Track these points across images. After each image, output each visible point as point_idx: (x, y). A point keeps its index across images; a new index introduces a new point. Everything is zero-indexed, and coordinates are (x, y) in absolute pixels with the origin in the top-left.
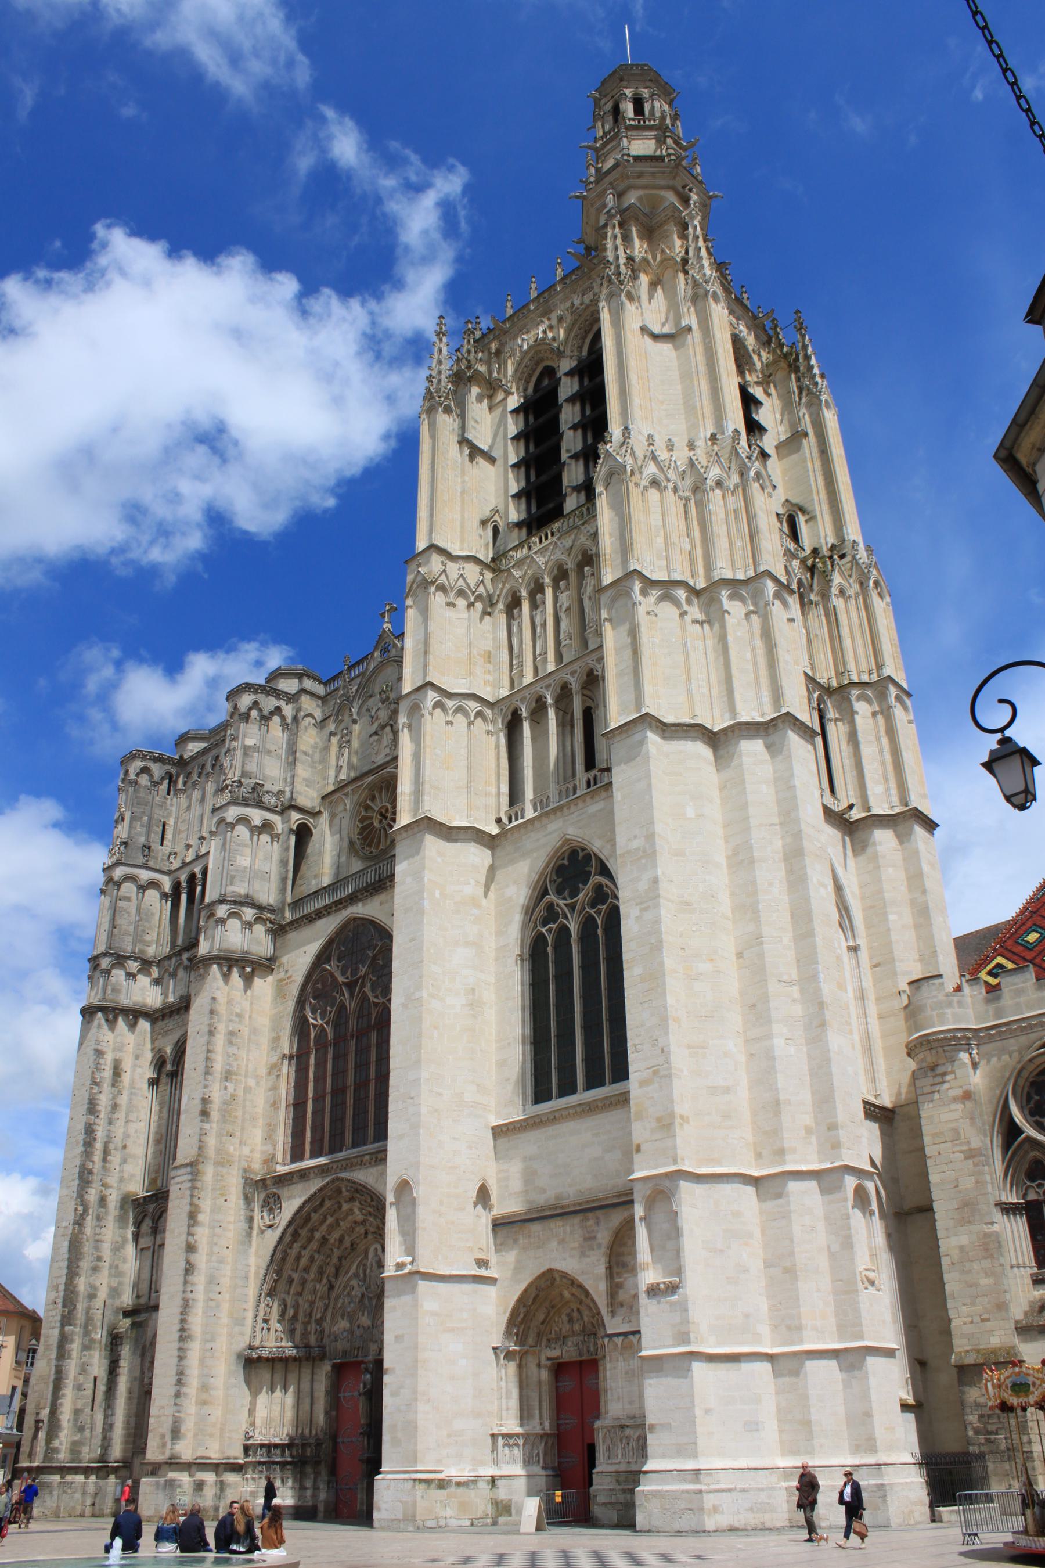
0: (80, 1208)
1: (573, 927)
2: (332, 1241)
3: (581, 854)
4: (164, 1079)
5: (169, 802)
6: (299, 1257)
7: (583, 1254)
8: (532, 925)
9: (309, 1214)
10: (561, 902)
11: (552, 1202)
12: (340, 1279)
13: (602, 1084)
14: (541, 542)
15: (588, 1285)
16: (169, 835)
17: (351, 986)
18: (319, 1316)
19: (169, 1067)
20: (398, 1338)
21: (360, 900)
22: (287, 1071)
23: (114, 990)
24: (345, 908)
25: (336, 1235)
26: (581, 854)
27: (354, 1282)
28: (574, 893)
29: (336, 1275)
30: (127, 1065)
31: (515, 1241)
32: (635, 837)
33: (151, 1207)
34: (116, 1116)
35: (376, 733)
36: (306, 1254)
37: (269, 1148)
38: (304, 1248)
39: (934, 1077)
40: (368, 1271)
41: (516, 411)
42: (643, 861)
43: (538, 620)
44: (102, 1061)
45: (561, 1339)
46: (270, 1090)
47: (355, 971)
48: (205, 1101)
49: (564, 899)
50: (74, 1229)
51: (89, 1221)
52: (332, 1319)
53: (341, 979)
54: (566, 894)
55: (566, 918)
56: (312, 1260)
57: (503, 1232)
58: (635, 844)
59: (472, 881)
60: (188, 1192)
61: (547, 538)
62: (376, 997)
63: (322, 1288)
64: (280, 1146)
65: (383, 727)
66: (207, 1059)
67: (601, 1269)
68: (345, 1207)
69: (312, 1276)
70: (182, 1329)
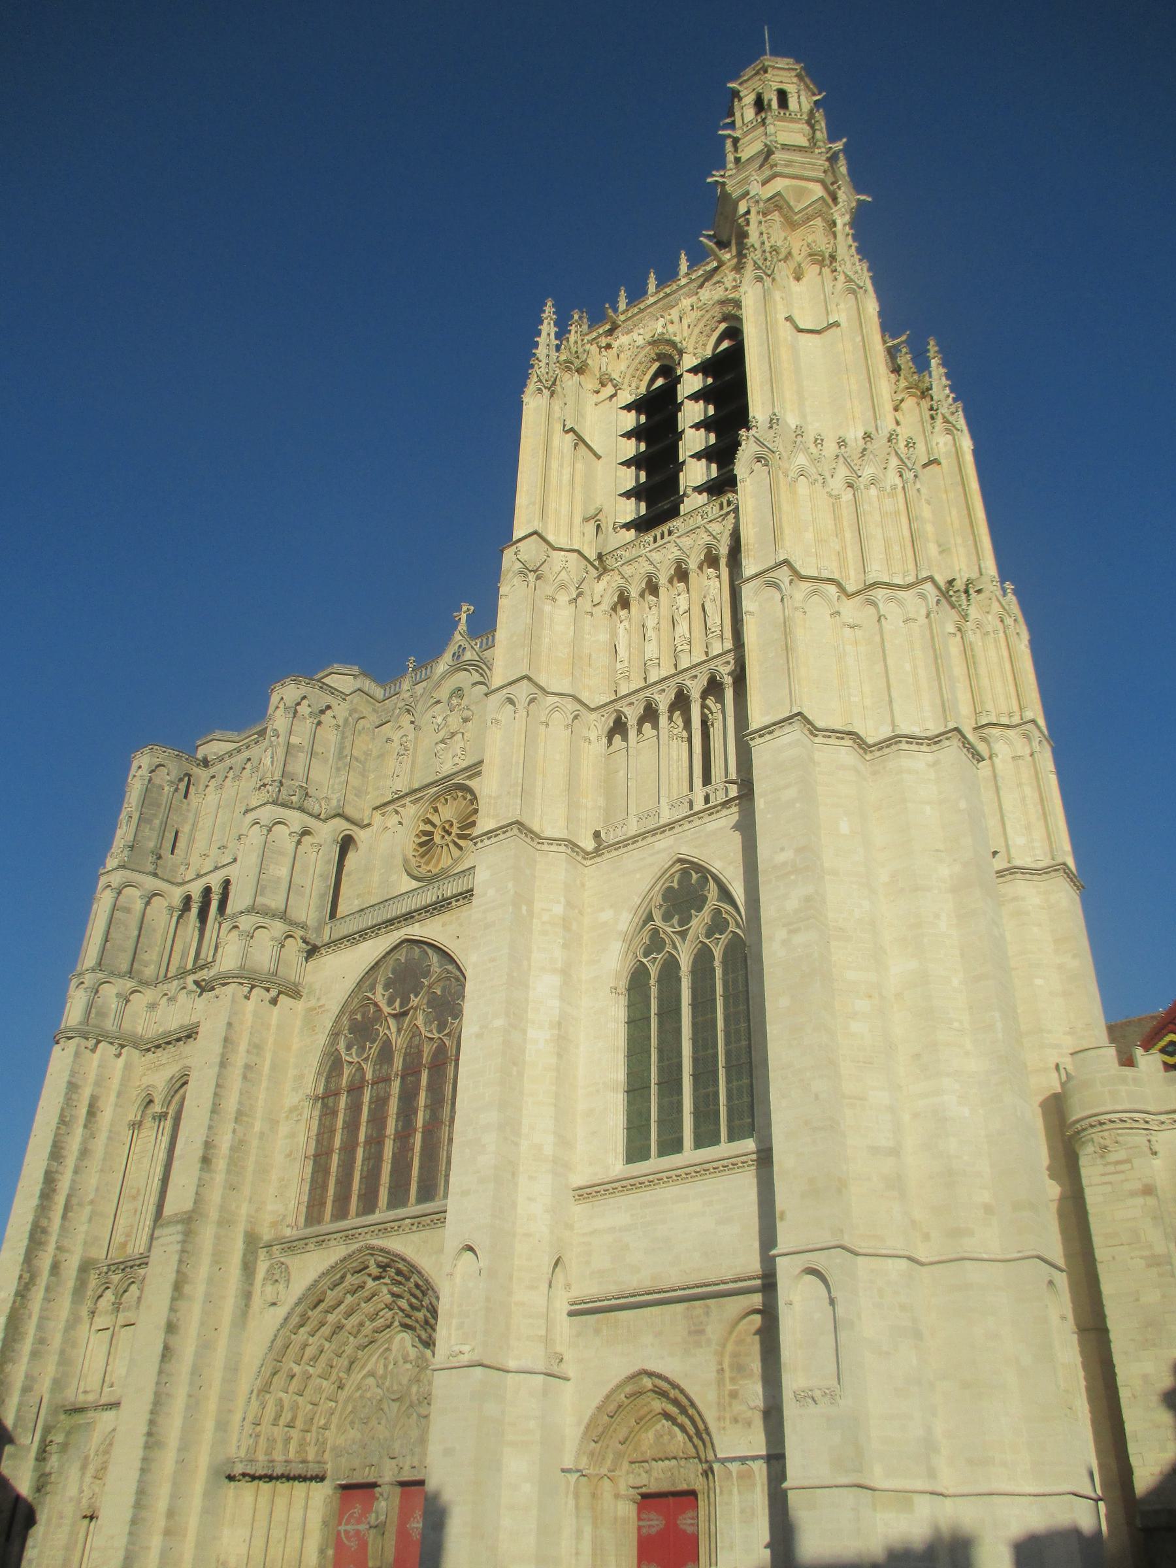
0: (26, 1276)
2: (348, 1327)
4: (149, 1123)
5: (185, 807)
6: (305, 1346)
9: (324, 1293)
10: (669, 930)
11: (648, 1284)
12: (353, 1376)
14: (655, 541)
16: (181, 844)
17: (399, 1016)
18: (322, 1422)
19: (157, 1108)
20: (448, 1452)
23: (98, 1014)
27: (371, 1381)
29: (349, 1369)
32: (782, 849)
33: (116, 1278)
34: (85, 1163)
35: (442, 742)
39: (1105, 1165)
40: (391, 1367)
41: (628, 408)
42: (793, 877)
43: (651, 623)
44: (74, 1096)
47: (405, 1001)
48: (208, 1145)
50: (14, 1302)
51: (38, 1295)
52: (339, 1427)
53: (387, 1010)
55: (675, 947)
58: (781, 857)
59: (562, 899)
60: (176, 1257)
61: (662, 537)
62: (431, 1031)
64: (292, 1205)
65: (453, 735)
66: (216, 1094)
69: (319, 1371)
70: (149, 1434)
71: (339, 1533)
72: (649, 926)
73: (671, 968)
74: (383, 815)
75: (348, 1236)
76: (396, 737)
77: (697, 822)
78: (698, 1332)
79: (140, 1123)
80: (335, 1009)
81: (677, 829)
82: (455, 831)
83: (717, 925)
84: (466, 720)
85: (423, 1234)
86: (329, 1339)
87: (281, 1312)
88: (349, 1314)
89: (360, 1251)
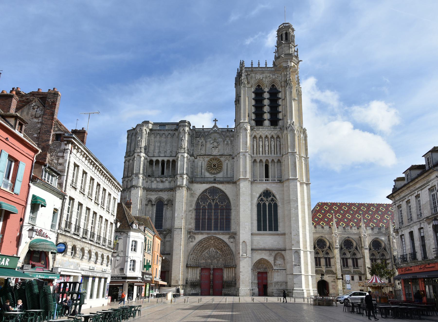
1: (267, 204)
4: (150, 205)
7: (269, 257)
11: (263, 248)
17: (213, 200)
21: (216, 184)
22: (194, 212)
25: (205, 245)
26: (269, 192)
28: (267, 198)
31: (255, 253)
36: (199, 248)
37: (190, 227)
38: (199, 247)
45: (260, 269)
46: (190, 215)
52: (201, 260)
56: (200, 249)
58: (294, 199)
63: (199, 254)
67: (273, 259)
68: (210, 241)
69: (199, 252)
71: (201, 274)
73: (265, 205)
74: (199, 157)
75: (208, 234)
76: (201, 141)
77: (271, 184)
78: (271, 254)
79: (147, 205)
80: (198, 195)
83: (272, 200)
84: (218, 145)
85: (224, 236)
86: (201, 248)
87: (194, 243)
88: (205, 244)
89: (211, 236)
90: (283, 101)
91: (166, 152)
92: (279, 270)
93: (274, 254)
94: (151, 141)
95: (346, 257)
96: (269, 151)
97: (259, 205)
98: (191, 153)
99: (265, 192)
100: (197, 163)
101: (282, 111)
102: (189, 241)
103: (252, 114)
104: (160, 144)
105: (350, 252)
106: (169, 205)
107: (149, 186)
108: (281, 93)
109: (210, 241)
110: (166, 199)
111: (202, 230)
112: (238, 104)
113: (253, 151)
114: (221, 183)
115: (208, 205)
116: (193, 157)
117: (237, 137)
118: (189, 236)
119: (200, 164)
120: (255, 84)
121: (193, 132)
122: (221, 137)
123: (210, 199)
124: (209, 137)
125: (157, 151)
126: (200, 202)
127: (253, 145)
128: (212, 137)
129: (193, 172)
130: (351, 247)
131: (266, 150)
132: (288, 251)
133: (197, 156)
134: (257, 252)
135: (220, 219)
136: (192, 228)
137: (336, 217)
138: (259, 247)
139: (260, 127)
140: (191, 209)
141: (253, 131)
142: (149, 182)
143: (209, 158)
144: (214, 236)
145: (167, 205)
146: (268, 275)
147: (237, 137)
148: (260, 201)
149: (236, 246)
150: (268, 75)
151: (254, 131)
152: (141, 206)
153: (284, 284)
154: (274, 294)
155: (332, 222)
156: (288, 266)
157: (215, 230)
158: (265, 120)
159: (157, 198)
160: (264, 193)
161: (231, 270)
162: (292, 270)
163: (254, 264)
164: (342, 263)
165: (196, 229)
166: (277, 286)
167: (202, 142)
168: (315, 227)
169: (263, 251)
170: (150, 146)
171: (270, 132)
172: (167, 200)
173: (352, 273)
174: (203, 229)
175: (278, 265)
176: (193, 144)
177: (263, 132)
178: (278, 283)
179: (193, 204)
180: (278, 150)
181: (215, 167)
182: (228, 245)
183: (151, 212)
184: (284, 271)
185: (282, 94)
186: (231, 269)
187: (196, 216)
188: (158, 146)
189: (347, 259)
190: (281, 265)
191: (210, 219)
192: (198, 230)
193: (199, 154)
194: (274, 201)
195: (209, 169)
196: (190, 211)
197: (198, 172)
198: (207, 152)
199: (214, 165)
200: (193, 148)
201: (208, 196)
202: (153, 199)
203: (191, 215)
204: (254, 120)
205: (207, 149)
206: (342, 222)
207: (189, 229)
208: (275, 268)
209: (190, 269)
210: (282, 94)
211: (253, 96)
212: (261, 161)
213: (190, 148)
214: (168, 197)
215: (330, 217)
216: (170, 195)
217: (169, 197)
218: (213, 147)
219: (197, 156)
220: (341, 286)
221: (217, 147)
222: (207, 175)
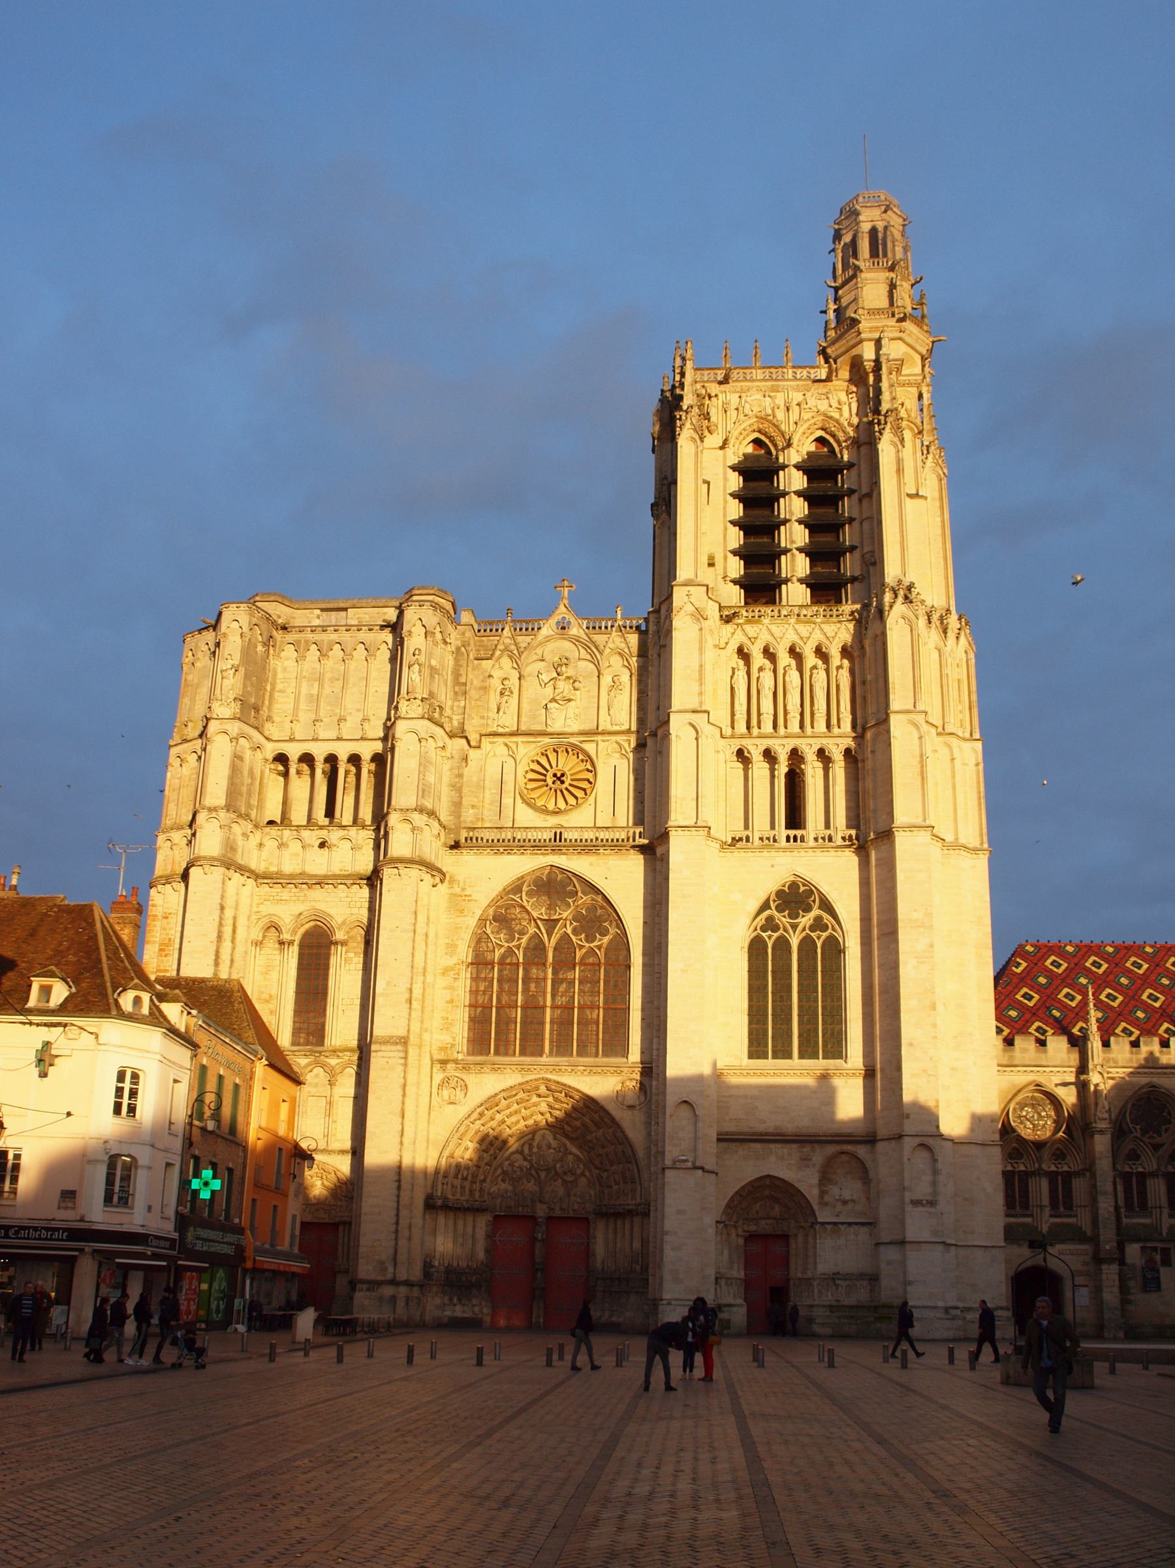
1: (795, 942)
3: (802, 889)
4: (271, 944)
8: (752, 928)
10: (783, 919)
11: (771, 1130)
13: (815, 1056)
15: (803, 1188)
21: (564, 854)
24: (542, 854)
30: (242, 922)
37: (446, 1038)
46: (445, 988)
49: (784, 917)
54: (786, 913)
57: (725, 1144)
62: (581, 940)
64: (459, 1039)
67: (815, 1180)
72: (768, 912)
73: (783, 945)
75: (522, 1068)
76: (497, 674)
78: (805, 1160)
79: (261, 943)
81: (795, 853)
82: (568, 782)
83: (818, 925)
87: (463, 1110)
89: (536, 1080)
90: (865, 503)
91: (345, 720)
92: (842, 1227)
93: (819, 1156)
94: (280, 676)
95: (1140, 1170)
96: (802, 714)
97: (756, 948)
98: (455, 723)
99: (786, 889)
100: (482, 769)
101: (862, 542)
102: (439, 1099)
103: (725, 557)
104: (321, 686)
105: (1156, 1147)
106: (352, 944)
107: (271, 864)
108: (856, 468)
109: (535, 1099)
110: (340, 920)
111: (497, 1053)
112: (664, 516)
113: (733, 714)
114: (588, 847)
115: (526, 949)
116: (464, 741)
117: (659, 655)
118: (438, 1077)
119: (493, 771)
120: (741, 434)
121: (463, 634)
122: (589, 657)
123: (535, 920)
124: (535, 657)
125: (305, 717)
126: (489, 931)
127: (732, 688)
128: (547, 656)
129: (460, 803)
130: (1164, 1127)
131: (789, 707)
132: (885, 1143)
133: (481, 735)
134: (743, 1150)
135: (581, 1008)
136: (453, 1045)
137: (1099, 1005)
138: (751, 1128)
139: (768, 610)
140: (451, 961)
141: (729, 628)
142: (271, 845)
143: (533, 745)
144: (549, 1080)
145: (344, 943)
146: (793, 1246)
147: (659, 655)
148: (764, 929)
149: (648, 1124)
150: (797, 397)
151: (738, 625)
152: (233, 949)
153: (865, 1283)
154: (816, 1328)
155: (1080, 1024)
156: (886, 1209)
157: (557, 1055)
158: (786, 581)
159: (300, 914)
160: (780, 894)
161: (627, 1226)
162: (902, 1223)
163: (732, 1200)
164: (1121, 1195)
165: (472, 1052)
166: (829, 1293)
167: (505, 679)
168: (1009, 1042)
169: (772, 1146)
170: (276, 694)
171: (804, 630)
172: (344, 923)
173: (1164, 1235)
174: (503, 1048)
175: (839, 1207)
176: (465, 684)
177: (774, 628)
178: (838, 1282)
179: (459, 943)
180: (842, 709)
181: (563, 782)
182: (613, 1120)
183: (274, 975)
184: (864, 1229)
185: (859, 475)
186: (627, 1222)
187: (474, 992)
188: (312, 696)
189: (1142, 1177)
190: (850, 1206)
191: (533, 1008)
192: (481, 1054)
193: (490, 730)
194: (824, 928)
195: (534, 795)
196: (445, 971)
197: (485, 805)
198: (524, 719)
199: (555, 775)
200: (462, 704)
201: (529, 908)
202: (287, 921)
203: (451, 988)
204: (735, 582)
205: (525, 706)
206: (1123, 1024)
207: (441, 1049)
208: (823, 1216)
209: (442, 1220)
210: (859, 475)
211: (735, 482)
212: (769, 756)
213: (449, 703)
214: (348, 911)
215: (1073, 1004)
216: (358, 904)
217: (355, 911)
218: (554, 700)
219: (481, 735)
220: (1116, 1290)
221: (569, 700)
222: (526, 816)
